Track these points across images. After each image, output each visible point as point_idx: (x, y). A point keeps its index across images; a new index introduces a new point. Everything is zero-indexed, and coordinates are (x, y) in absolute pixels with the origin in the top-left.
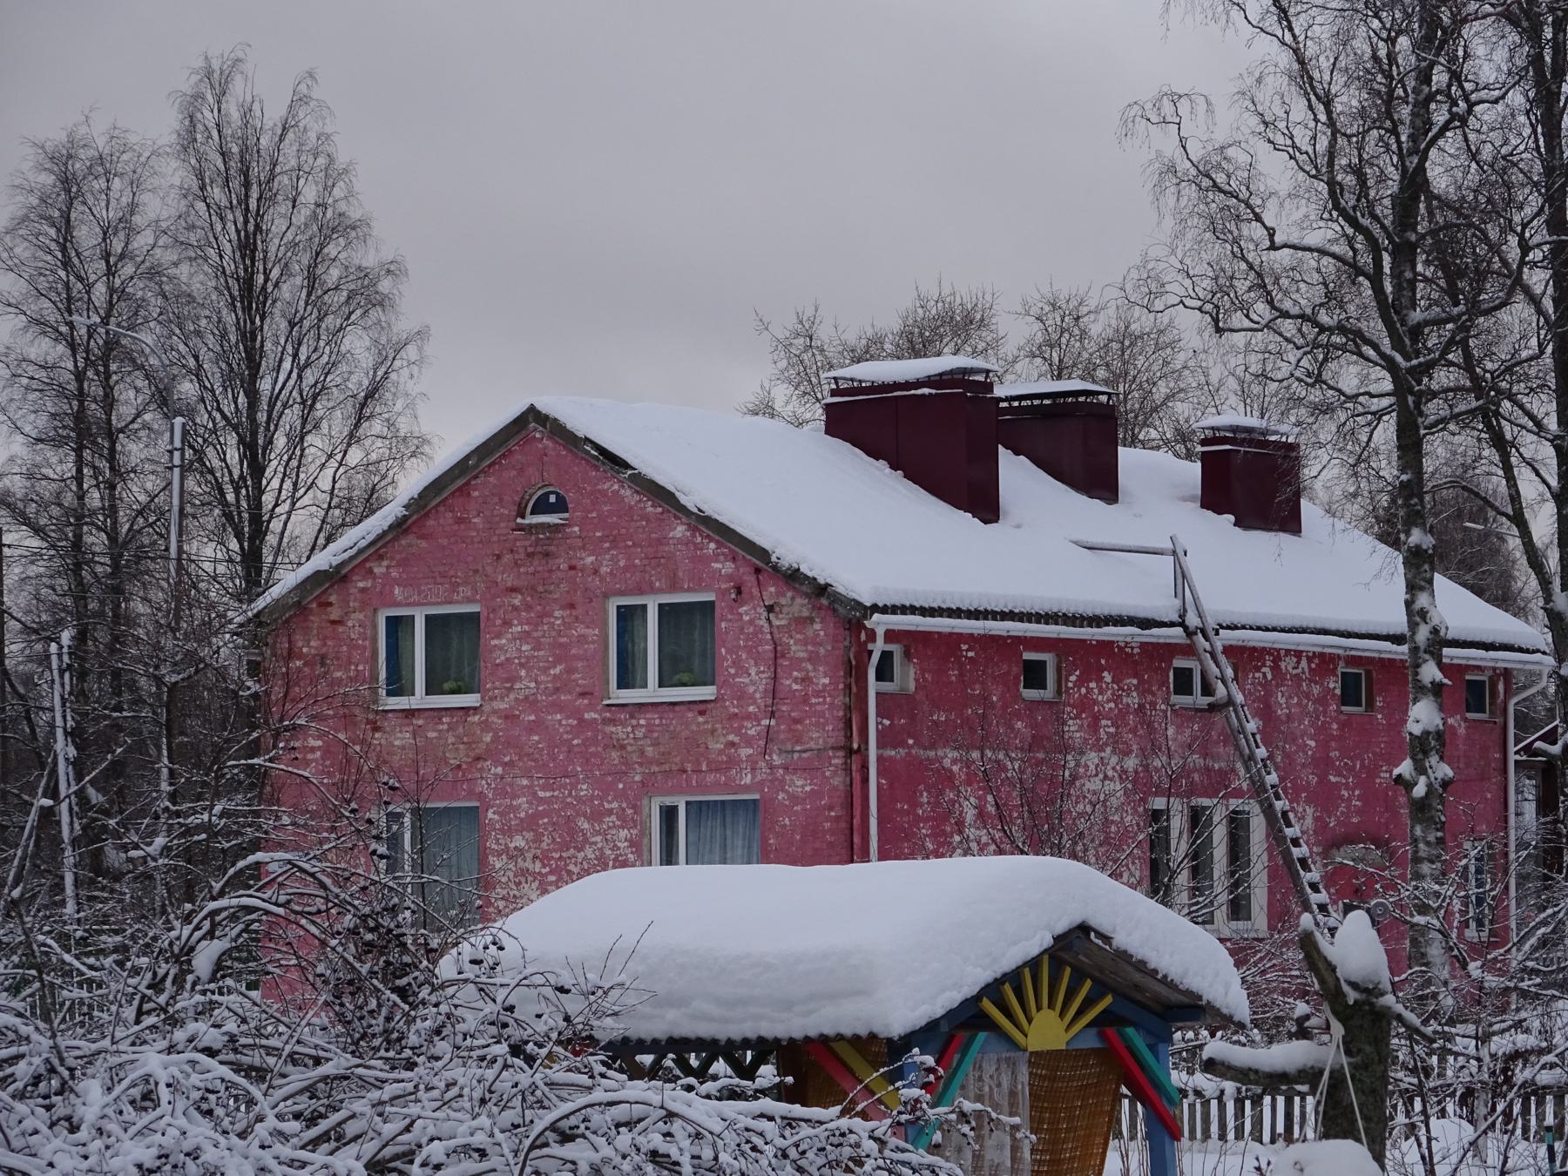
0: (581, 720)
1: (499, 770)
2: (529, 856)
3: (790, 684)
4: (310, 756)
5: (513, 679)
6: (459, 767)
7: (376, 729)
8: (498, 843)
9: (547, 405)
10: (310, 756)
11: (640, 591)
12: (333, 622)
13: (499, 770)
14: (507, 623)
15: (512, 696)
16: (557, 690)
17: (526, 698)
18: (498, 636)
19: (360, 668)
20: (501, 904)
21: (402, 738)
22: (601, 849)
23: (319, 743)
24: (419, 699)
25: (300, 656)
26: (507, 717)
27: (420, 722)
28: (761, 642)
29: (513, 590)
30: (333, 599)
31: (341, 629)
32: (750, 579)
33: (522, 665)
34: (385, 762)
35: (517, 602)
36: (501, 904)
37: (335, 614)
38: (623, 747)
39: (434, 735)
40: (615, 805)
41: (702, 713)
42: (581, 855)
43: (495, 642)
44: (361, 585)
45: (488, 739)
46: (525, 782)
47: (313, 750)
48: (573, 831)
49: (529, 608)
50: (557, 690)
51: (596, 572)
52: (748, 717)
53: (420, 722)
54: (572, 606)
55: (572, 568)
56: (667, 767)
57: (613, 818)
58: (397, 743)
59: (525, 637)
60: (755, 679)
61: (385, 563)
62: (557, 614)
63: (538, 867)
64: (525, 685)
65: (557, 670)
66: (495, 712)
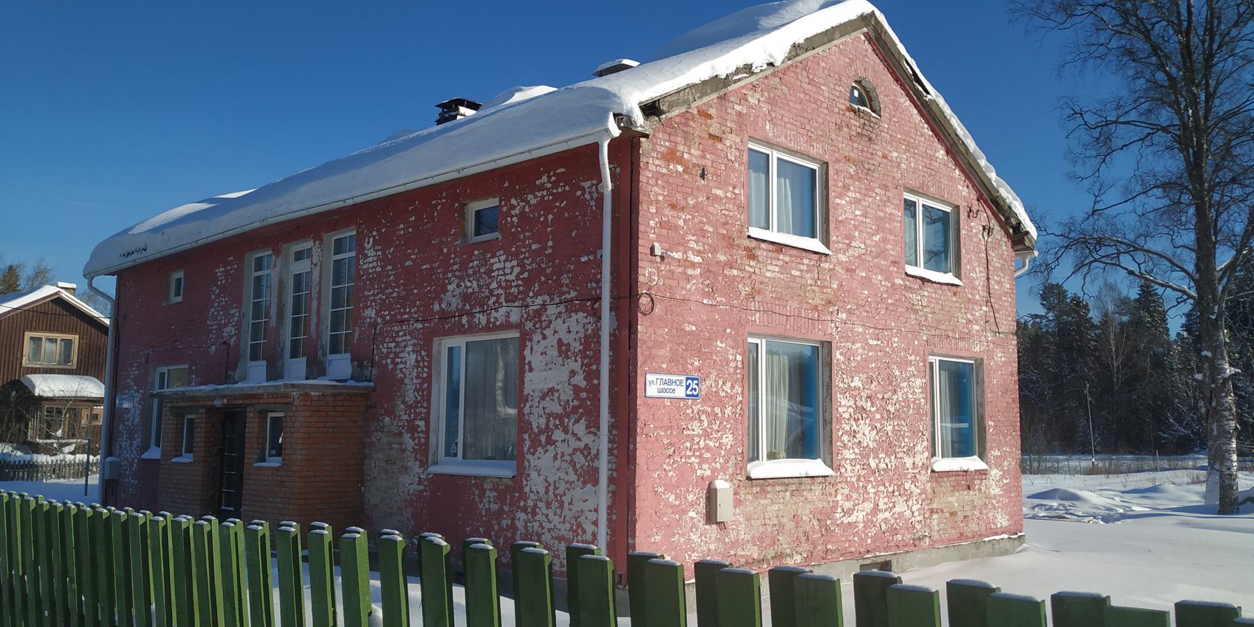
0: (893, 285)
1: (844, 316)
2: (864, 395)
3: (995, 286)
4: (690, 272)
6: (816, 308)
8: (843, 382)
10: (690, 272)
12: (712, 136)
13: (844, 316)
14: (846, 187)
15: (851, 252)
17: (859, 256)
18: (840, 196)
19: (737, 191)
20: (845, 438)
21: (772, 271)
22: (906, 393)
23: (698, 259)
25: (680, 161)
26: (847, 270)
29: (848, 159)
30: (712, 111)
31: (719, 146)
33: (856, 228)
35: (851, 171)
36: (845, 438)
38: (916, 312)
39: (797, 273)
40: (913, 358)
41: (955, 294)
42: (895, 397)
43: (838, 201)
44: (738, 108)
45: (835, 286)
46: (860, 330)
47: (693, 265)
48: (890, 378)
49: (860, 179)
51: (899, 165)
52: (976, 303)
53: (787, 259)
54: (885, 188)
55: (885, 157)
56: (938, 332)
57: (913, 368)
59: (857, 202)
60: (978, 275)
61: (757, 96)
62: (878, 190)
65: (877, 238)
66: (840, 263)
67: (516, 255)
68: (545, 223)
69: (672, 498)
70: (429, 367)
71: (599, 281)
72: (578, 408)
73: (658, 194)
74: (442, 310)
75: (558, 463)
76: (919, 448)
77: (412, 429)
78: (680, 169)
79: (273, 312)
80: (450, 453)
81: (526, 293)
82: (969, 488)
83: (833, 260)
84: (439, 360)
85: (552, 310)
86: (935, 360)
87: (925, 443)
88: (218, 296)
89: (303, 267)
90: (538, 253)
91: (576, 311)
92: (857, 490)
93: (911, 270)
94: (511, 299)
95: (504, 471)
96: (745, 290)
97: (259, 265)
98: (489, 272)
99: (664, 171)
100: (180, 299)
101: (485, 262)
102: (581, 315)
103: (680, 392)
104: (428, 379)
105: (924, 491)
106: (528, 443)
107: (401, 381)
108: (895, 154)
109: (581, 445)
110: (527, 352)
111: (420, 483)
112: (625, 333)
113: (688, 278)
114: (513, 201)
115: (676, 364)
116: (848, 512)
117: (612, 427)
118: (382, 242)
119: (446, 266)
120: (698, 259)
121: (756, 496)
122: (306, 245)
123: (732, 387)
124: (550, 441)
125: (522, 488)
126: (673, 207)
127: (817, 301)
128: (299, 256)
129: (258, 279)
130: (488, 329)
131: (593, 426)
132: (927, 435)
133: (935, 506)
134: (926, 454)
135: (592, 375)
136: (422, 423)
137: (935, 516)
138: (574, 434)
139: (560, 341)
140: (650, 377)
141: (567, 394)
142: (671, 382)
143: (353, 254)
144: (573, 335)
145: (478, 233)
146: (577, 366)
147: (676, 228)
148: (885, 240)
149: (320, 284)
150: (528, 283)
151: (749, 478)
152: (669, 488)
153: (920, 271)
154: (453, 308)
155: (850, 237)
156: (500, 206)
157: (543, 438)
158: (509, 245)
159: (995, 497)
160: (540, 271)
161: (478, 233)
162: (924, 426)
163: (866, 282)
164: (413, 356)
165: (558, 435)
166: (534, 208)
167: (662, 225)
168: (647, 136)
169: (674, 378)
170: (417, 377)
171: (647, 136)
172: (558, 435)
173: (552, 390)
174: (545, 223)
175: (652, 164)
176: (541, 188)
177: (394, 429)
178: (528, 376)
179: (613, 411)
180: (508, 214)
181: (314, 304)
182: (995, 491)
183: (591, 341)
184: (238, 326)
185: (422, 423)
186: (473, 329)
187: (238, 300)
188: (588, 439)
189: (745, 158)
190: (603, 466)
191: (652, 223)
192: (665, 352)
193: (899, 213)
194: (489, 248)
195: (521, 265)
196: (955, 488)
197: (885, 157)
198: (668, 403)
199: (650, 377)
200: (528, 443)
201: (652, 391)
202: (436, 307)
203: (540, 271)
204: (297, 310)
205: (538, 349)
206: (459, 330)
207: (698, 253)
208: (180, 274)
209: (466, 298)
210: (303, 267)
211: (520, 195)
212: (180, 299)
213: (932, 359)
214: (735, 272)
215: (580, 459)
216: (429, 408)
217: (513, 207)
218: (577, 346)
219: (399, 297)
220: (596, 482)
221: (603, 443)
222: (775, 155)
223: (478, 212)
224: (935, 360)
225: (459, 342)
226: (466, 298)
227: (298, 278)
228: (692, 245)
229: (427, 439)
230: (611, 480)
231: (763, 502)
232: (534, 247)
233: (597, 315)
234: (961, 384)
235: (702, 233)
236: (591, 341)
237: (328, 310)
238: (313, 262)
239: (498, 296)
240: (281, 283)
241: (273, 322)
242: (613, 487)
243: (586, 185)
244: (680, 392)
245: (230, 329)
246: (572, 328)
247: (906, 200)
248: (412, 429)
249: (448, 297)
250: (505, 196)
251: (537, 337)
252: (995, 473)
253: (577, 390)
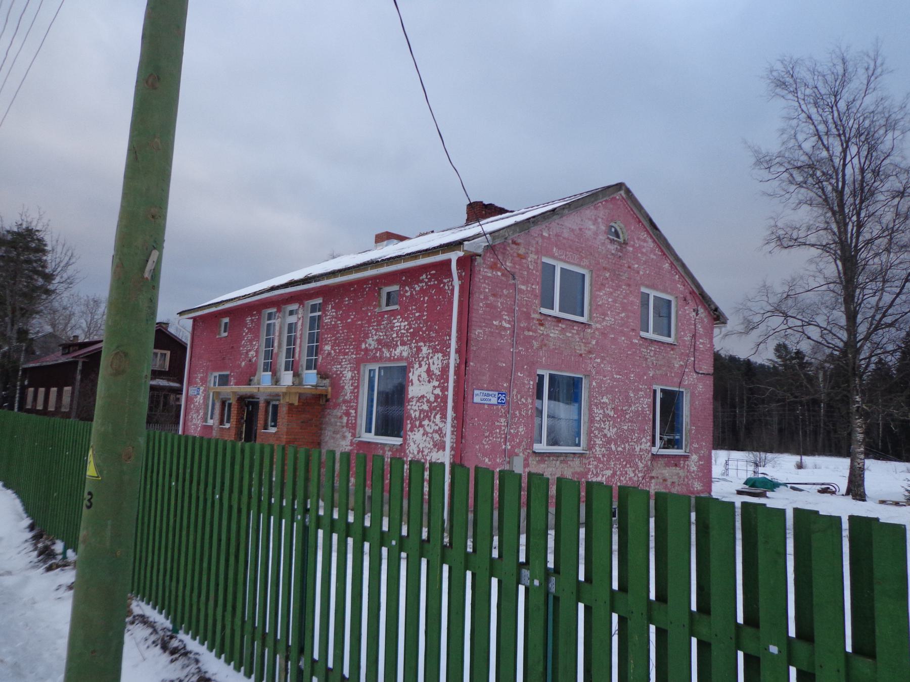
0: (632, 342)
1: (599, 360)
2: (609, 407)
5: (605, 315)
6: (581, 355)
7: (542, 325)
9: (629, 185)
11: (653, 287)
12: (519, 255)
16: (622, 325)
18: (600, 290)
20: (596, 432)
21: (554, 333)
24: (556, 312)
25: (500, 269)
26: (603, 333)
27: (564, 326)
28: (691, 324)
29: (605, 269)
32: (689, 297)
33: (609, 309)
34: (545, 345)
35: (607, 275)
36: (596, 432)
37: (522, 251)
41: (672, 349)
43: (598, 293)
48: (627, 397)
49: (612, 280)
50: (622, 325)
51: (638, 273)
53: (564, 326)
54: (629, 285)
55: (629, 267)
58: (552, 335)
63: (612, 414)
64: (609, 320)
66: (597, 329)
67: (406, 319)
68: (423, 302)
69: (487, 460)
70: (358, 380)
71: (450, 336)
72: (436, 407)
73: (485, 288)
74: (366, 348)
75: (424, 438)
76: (644, 440)
77: (347, 414)
78: (499, 274)
79: (276, 344)
80: (369, 430)
81: (411, 340)
82: (676, 465)
83: (594, 326)
84: (364, 376)
86: (658, 388)
87: (648, 438)
88: (247, 334)
89: (292, 319)
90: (419, 318)
91: (438, 352)
92: (602, 463)
93: (643, 334)
95: (397, 441)
96: (536, 344)
97: (270, 316)
99: (490, 275)
100: (226, 334)
101: (391, 322)
102: (440, 355)
103: (494, 401)
104: (357, 387)
105: (646, 466)
106: (409, 426)
107: (343, 387)
108: (636, 266)
109: (437, 428)
111: (351, 445)
112: (463, 366)
113: (502, 337)
114: (407, 288)
115: (493, 386)
116: (597, 475)
117: (455, 418)
118: (337, 307)
119: (369, 322)
120: (508, 326)
121: (539, 462)
122: (294, 307)
123: (526, 400)
124: (421, 426)
125: (405, 452)
126: (494, 295)
127: (582, 352)
128: (291, 313)
129: (269, 325)
130: (390, 360)
131: (444, 417)
132: (650, 433)
133: (653, 474)
134: (649, 444)
135: (444, 389)
136: (353, 412)
137: (653, 481)
138: (434, 422)
140: (476, 392)
142: (489, 395)
143: (320, 313)
144: (436, 366)
145: (387, 305)
147: (496, 307)
148: (628, 317)
149: (301, 330)
150: (413, 335)
151: (534, 452)
152: (485, 455)
153: (650, 335)
154: (372, 347)
155: (605, 315)
156: (400, 291)
157: (417, 423)
158: (402, 313)
159: (693, 472)
160: (420, 329)
161: (387, 305)
162: (648, 427)
163: (614, 340)
166: (418, 293)
167: (487, 306)
168: (480, 256)
169: (491, 393)
170: (352, 385)
171: (480, 256)
172: (426, 422)
173: (423, 397)
174: (423, 302)
175: (483, 271)
176: (422, 281)
179: (455, 409)
180: (404, 295)
181: (298, 341)
182: (694, 468)
183: (445, 370)
184: (257, 352)
185: (353, 412)
186: (380, 359)
187: (257, 337)
188: (441, 425)
189: (540, 268)
190: (449, 440)
191: (481, 304)
192: (486, 378)
193: (638, 302)
194: (393, 313)
195: (409, 324)
196: (667, 465)
197: (629, 267)
198: (486, 407)
199: (476, 392)
200: (409, 426)
201: (477, 399)
202: (363, 346)
203: (420, 329)
204: (289, 343)
205: (417, 373)
206: (375, 359)
207: (509, 322)
208: (226, 320)
209: (379, 341)
210: (292, 319)
211: (411, 286)
212: (226, 334)
213: (655, 387)
214: (531, 333)
215: (436, 436)
216: (357, 403)
217: (406, 292)
218: (438, 372)
220: (444, 450)
221: (448, 429)
222: (559, 266)
223: (389, 294)
224: (658, 388)
225: (375, 366)
227: (290, 325)
228: (505, 317)
229: (356, 420)
230: (452, 448)
231: (542, 466)
232: (417, 314)
233: (446, 354)
234: (670, 403)
235: (511, 311)
236: (445, 370)
237: (306, 345)
238: (298, 317)
239: (397, 342)
240: (281, 328)
241: (276, 350)
242: (453, 453)
243: (445, 281)
244: (494, 401)
245: (252, 353)
247: (643, 293)
249: (370, 341)
250: (403, 285)
251: (416, 366)
252: (694, 457)
253: (437, 397)
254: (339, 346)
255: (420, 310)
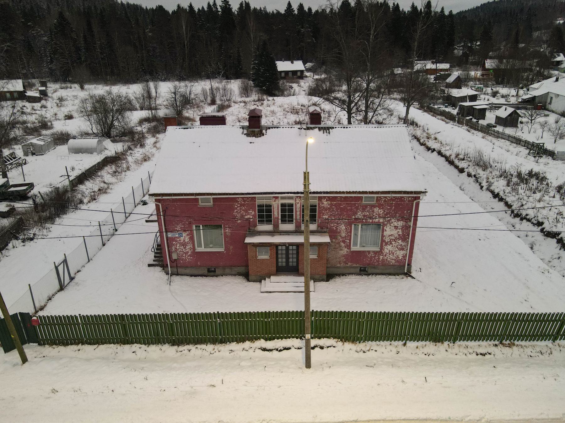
67: (382, 209)
85: (393, 220)
94: (380, 217)
98: (373, 211)
110: (385, 228)
124: (391, 243)
139: (395, 226)
141: (396, 235)
146: (400, 231)
164: (344, 227)
165: (393, 243)
172: (393, 243)
177: (337, 241)
178: (385, 232)
185: (348, 241)
188: (402, 243)
202: (353, 217)
209: (364, 216)
219: (338, 214)
226: (364, 216)
246: (401, 223)
248: (344, 242)
253: (399, 235)
254: (334, 216)
255: (391, 205)
